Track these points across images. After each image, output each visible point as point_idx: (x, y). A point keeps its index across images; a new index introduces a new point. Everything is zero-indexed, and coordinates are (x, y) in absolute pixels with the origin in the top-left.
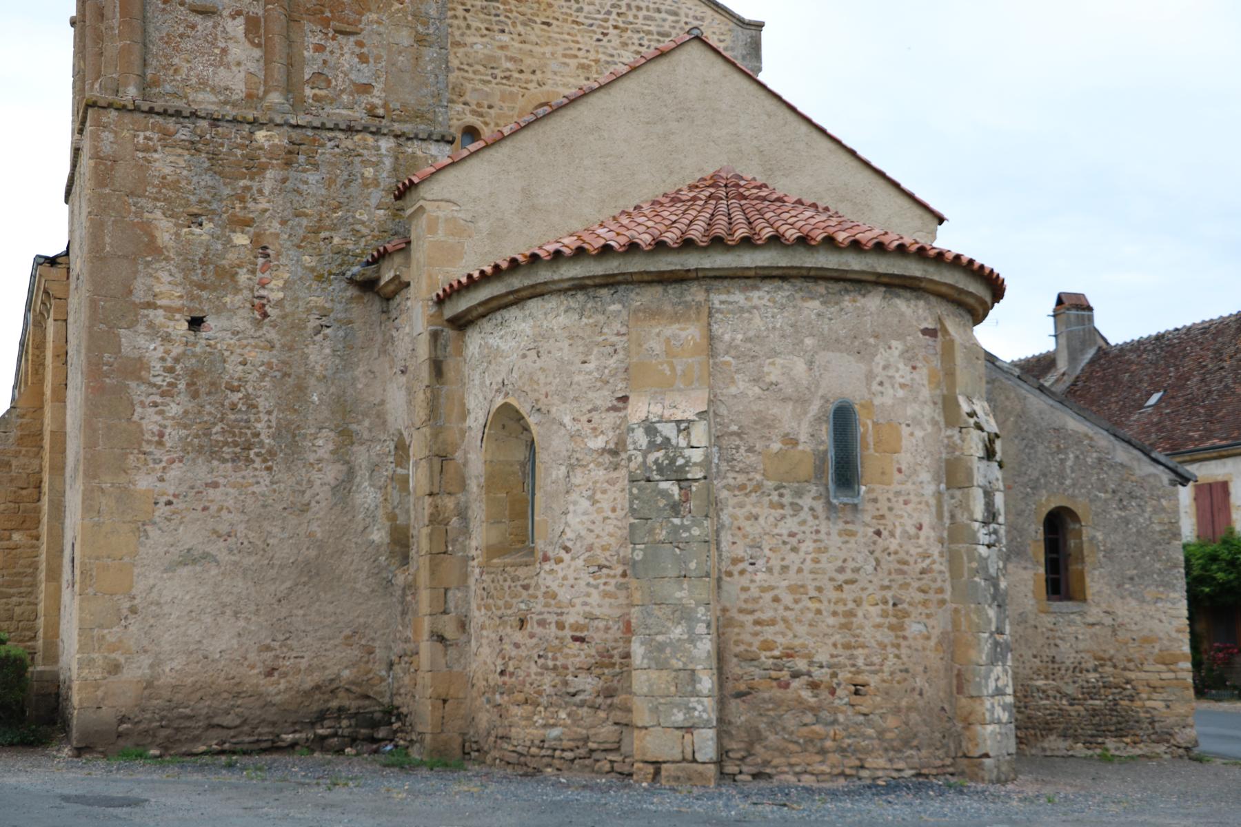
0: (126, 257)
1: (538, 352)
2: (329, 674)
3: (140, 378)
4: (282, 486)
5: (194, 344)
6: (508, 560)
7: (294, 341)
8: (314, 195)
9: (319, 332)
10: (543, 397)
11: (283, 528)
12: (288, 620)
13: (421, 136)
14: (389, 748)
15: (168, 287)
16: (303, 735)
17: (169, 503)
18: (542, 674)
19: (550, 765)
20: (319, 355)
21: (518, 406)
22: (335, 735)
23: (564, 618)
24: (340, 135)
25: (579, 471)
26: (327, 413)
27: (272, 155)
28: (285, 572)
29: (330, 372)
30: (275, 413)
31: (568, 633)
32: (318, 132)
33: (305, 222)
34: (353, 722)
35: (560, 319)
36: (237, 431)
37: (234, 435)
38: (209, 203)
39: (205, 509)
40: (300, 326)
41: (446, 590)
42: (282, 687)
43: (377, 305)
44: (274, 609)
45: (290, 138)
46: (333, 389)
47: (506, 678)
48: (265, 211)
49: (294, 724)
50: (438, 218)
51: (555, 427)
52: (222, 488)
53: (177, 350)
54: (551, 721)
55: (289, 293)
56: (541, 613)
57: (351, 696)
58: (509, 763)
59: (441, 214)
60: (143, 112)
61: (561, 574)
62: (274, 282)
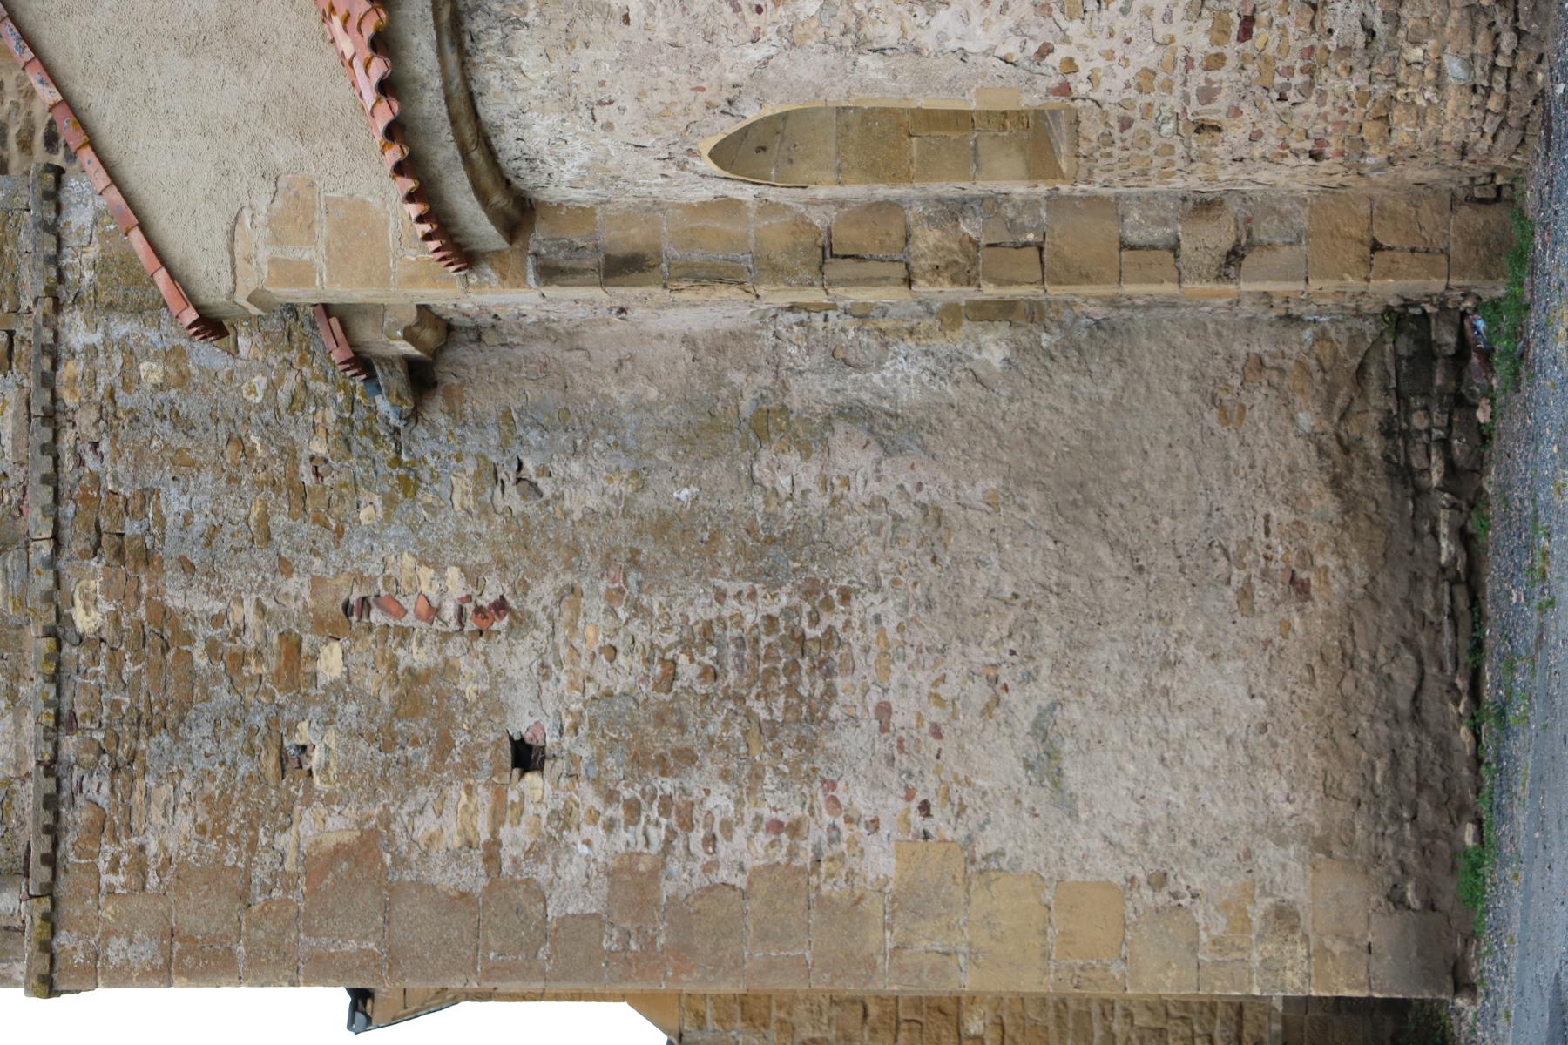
0: (387, 907)
1: (600, 103)
2: (1305, 457)
3: (653, 874)
4: (882, 565)
5: (574, 759)
6: (1064, 148)
7: (557, 542)
8: (216, 498)
9: (534, 485)
10: (702, 96)
11: (979, 563)
12: (1183, 550)
13: (52, 250)
14: (1481, 324)
16: (1444, 515)
17: (925, 808)
18: (1322, 94)
19: (1529, 77)
20: (586, 486)
21: (721, 137)
22: (1445, 444)
23: (1198, 57)
24: (68, 438)
25: (869, 30)
26: (718, 468)
27: (128, 595)
28: (1077, 558)
29: (623, 462)
30: (720, 582)
31: (1232, 48)
32: (65, 488)
33: (280, 520)
34: (1416, 402)
35: (526, 63)
36: (763, 666)
37: (772, 672)
38: (252, 731)
39: (937, 732)
40: (522, 530)
41: (1125, 246)
42: (1333, 562)
43: (464, 354)
44: (1159, 581)
45: (84, 555)
46: (663, 455)
47: (1328, 151)
48: (260, 608)
49: (1416, 535)
50: (273, 262)
51: (770, 75)
52: (891, 697)
53: (589, 797)
54: (1429, 74)
55: (448, 553)
56: (1186, 97)
57: (1356, 407)
58: (1523, 141)
59: (264, 254)
60: (54, 877)
61: (1100, 63)
62: (424, 588)
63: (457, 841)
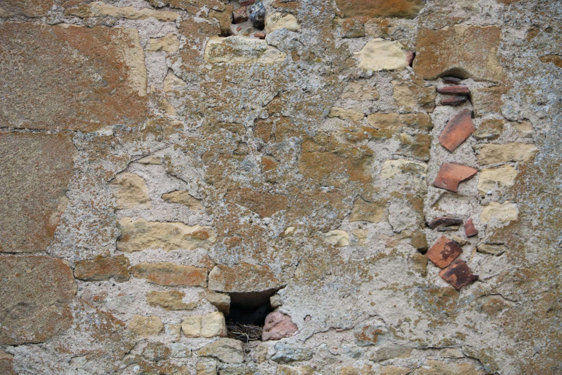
0: (37, 131)
15: (164, 211)
55: (538, 204)
62: (486, 174)
63: (127, 222)
